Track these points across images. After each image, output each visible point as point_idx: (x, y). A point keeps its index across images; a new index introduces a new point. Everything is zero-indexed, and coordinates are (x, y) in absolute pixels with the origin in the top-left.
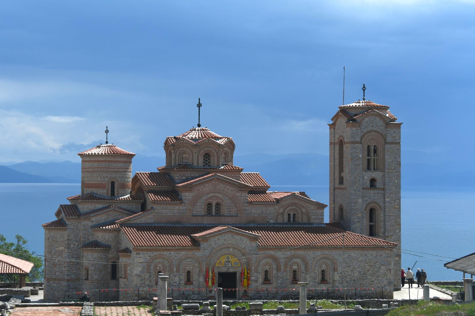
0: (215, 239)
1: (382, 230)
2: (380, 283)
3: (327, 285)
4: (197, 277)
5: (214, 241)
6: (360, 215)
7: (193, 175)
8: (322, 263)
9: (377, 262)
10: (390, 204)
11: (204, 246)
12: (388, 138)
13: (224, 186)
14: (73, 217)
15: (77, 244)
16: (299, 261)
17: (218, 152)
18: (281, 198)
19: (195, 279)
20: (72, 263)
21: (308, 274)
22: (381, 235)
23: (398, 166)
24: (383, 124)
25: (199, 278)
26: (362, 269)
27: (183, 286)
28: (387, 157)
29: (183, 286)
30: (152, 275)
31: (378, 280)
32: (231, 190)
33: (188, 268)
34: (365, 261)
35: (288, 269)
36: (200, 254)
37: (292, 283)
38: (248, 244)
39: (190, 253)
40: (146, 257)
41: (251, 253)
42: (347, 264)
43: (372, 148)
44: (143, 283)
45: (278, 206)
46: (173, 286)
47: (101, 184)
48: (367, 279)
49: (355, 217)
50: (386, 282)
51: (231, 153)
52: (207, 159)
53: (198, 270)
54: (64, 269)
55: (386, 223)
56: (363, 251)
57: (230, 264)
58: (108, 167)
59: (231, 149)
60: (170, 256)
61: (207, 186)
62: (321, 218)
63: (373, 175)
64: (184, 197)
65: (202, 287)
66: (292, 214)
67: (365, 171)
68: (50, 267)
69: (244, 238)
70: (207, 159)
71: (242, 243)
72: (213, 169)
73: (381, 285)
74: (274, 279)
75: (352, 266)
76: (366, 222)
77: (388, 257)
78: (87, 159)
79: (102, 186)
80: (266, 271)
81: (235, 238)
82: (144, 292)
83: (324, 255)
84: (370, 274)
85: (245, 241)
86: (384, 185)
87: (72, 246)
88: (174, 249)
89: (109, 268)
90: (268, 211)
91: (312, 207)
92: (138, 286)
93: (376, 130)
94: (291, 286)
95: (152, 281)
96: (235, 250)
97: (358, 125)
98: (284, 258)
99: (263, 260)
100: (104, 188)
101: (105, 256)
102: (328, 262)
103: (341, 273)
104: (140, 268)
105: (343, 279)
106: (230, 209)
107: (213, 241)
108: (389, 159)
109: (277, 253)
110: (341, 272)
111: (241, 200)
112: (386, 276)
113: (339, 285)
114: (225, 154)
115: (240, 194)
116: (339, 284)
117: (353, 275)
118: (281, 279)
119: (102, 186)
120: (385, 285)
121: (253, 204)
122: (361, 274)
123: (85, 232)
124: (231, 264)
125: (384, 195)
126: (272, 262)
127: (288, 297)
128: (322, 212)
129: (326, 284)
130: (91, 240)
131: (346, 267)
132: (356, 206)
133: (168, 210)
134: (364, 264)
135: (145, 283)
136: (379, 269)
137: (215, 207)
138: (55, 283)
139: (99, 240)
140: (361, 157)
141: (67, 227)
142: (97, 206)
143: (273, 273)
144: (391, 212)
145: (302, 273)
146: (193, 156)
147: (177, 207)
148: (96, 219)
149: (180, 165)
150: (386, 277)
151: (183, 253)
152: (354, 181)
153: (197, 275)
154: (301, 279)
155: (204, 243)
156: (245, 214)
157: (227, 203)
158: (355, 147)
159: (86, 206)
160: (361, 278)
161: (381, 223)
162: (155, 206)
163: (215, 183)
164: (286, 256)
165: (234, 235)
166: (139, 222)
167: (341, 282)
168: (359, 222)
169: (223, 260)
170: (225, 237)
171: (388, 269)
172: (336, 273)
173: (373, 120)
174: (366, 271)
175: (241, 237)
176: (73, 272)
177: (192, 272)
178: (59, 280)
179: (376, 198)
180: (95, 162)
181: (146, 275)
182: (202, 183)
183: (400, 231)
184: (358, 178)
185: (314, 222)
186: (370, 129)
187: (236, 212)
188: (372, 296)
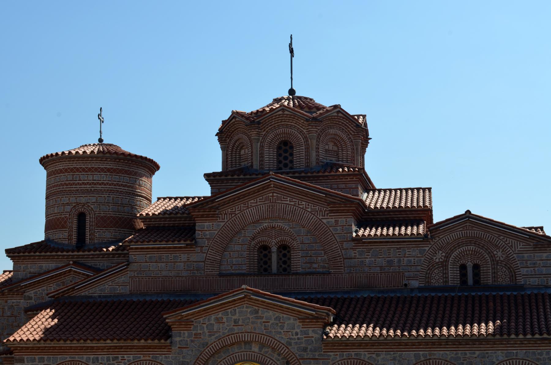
0: (209, 320)
5: (207, 327)
11: (182, 339)
13: (292, 203)
17: (308, 136)
36: (170, 360)
39: (148, 358)
41: (305, 357)
45: (430, 246)
47: (58, 219)
51: (352, 141)
58: (72, 182)
59: (351, 132)
61: (253, 205)
62: (544, 273)
64: (200, 232)
66: (470, 266)
69: (285, 316)
70: (287, 155)
71: (282, 329)
83: (514, 361)
90: (405, 259)
91: (520, 246)
96: (266, 350)
100: (63, 227)
106: (311, 256)
107: (205, 326)
109: (378, 355)
111: (335, 235)
114: (335, 143)
121: (364, 243)
123: (14, 322)
133: (163, 264)
137: (278, 255)
142: (44, 265)
148: (36, 293)
151: (128, 357)
155: (182, 332)
159: (22, 267)
162: (133, 256)
163: (273, 196)
165: (260, 309)
175: (277, 314)
187: (326, 265)
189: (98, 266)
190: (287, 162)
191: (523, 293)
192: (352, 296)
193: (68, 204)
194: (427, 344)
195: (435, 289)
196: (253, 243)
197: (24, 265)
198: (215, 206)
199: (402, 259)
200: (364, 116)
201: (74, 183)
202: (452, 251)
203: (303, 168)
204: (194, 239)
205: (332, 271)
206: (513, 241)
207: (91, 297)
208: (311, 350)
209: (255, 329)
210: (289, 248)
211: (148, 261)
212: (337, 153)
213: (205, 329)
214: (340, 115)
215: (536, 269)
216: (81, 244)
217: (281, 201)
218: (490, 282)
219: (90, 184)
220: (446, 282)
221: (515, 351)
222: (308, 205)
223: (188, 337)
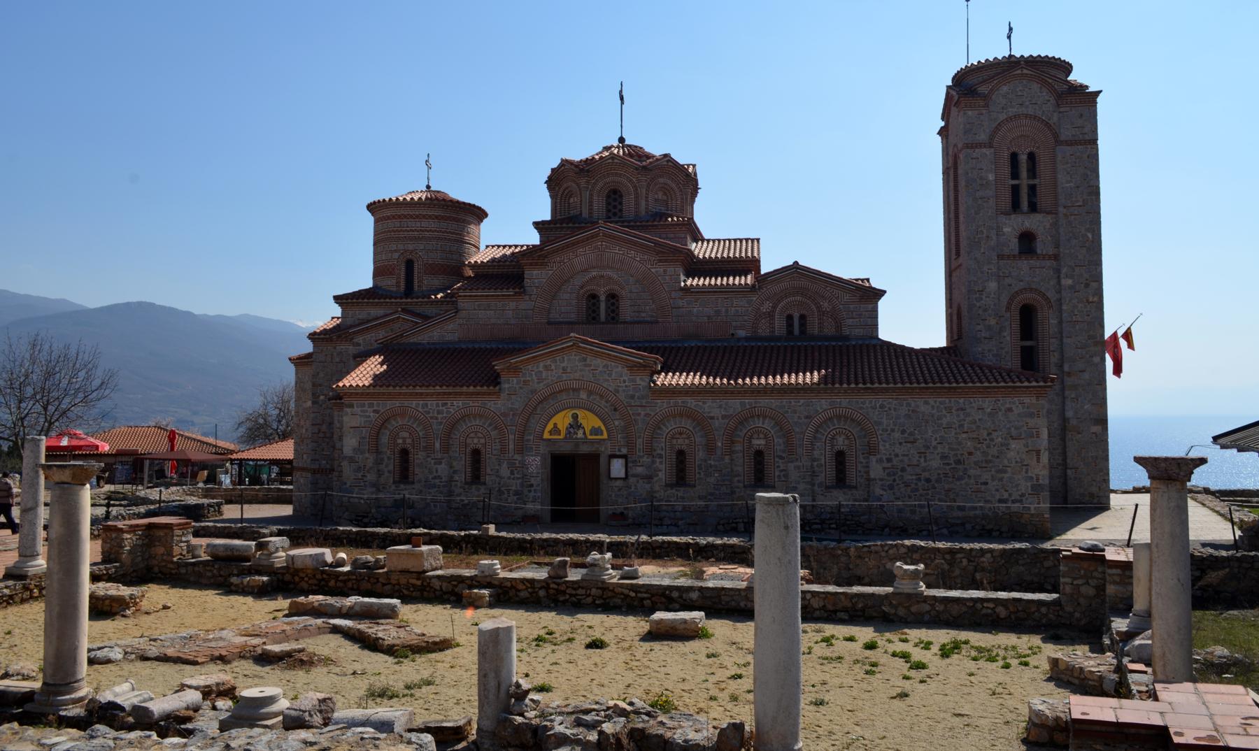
0: (538, 367)
1: (1054, 358)
2: (1007, 489)
3: (850, 493)
6: (993, 322)
9: (996, 431)
12: (1062, 131)
16: (767, 425)
20: (321, 435)
21: (792, 462)
26: (951, 449)
27: (461, 487)
29: (461, 487)
30: (386, 459)
33: (475, 442)
35: (738, 447)
36: (499, 406)
38: (624, 382)
39: (477, 404)
42: (906, 435)
43: (1023, 158)
46: (434, 486)
48: (966, 476)
49: (979, 327)
50: (1025, 486)
53: (499, 447)
55: (1065, 340)
56: (953, 400)
63: (1026, 223)
65: (506, 492)
66: (796, 316)
70: (617, 203)
73: (1010, 495)
74: (699, 473)
75: (920, 441)
77: (1031, 415)
80: (681, 453)
81: (590, 365)
82: (362, 501)
84: (976, 463)
85: (616, 372)
86: (1057, 246)
87: (322, 397)
90: (733, 309)
94: (748, 492)
95: (386, 474)
97: (982, 103)
98: (723, 419)
100: (391, 274)
103: (889, 460)
104: (354, 440)
105: (894, 474)
108: (1068, 182)
109: (704, 403)
110: (888, 456)
113: (881, 492)
116: (883, 489)
120: (1023, 495)
121: (692, 292)
122: (948, 464)
124: (584, 433)
125: (1058, 271)
126: (694, 428)
127: (736, 523)
132: (982, 299)
134: (956, 434)
135: (365, 479)
136: (1004, 448)
137: (606, 304)
145: (777, 459)
147: (513, 305)
150: (1027, 472)
152: (975, 238)
157: (631, 292)
158: (975, 155)
161: (1052, 340)
164: (731, 413)
167: (888, 483)
169: (562, 420)
170: (564, 361)
171: (1030, 448)
172: (873, 459)
173: (1021, 88)
175: (605, 362)
179: (1035, 280)
181: (367, 458)
184: (985, 231)
188: (983, 526)
190: (617, 211)
191: (848, 343)
192: (680, 345)
193: (395, 251)
194: (753, 392)
200: (694, 166)
202: (779, 302)
204: (523, 287)
207: (420, 344)
208: (638, 398)
209: (583, 377)
214: (670, 164)
216: (409, 291)
218: (816, 332)
220: (773, 332)
223: (517, 384)
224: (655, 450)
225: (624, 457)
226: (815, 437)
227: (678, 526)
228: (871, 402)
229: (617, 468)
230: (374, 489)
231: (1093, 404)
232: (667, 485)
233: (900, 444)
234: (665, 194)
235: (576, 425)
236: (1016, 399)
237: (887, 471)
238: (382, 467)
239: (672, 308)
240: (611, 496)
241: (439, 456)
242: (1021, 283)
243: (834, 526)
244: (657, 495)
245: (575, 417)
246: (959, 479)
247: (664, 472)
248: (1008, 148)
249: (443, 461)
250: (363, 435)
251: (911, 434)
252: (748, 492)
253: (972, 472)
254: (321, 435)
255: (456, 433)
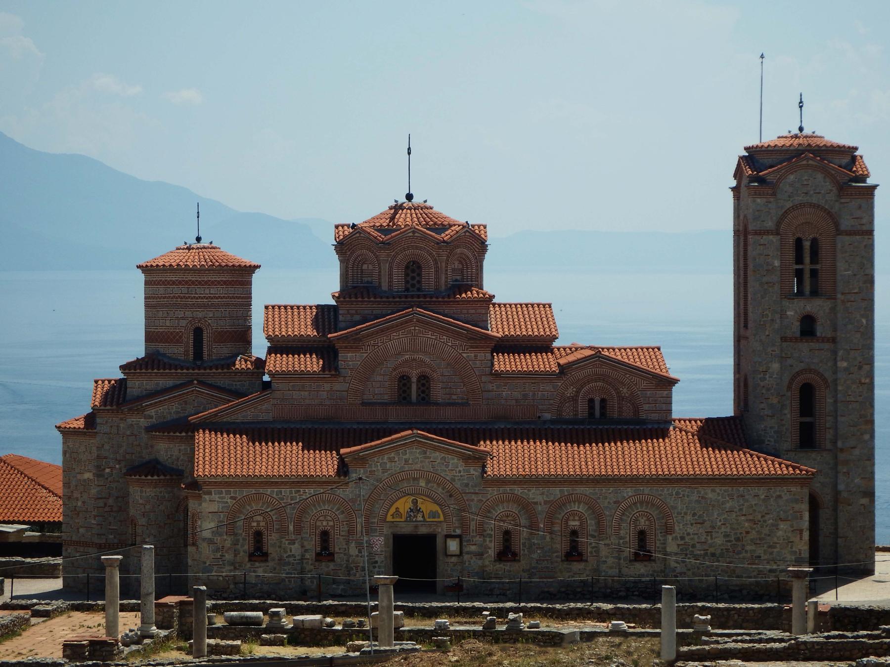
0: (382, 459)
4: (344, 544)
6: (775, 401)
7: (379, 312)
8: (637, 514)
9: (768, 514)
10: (849, 374)
14: (107, 408)
15: (117, 466)
18: (569, 363)
19: (340, 549)
20: (107, 509)
22: (829, 446)
23: (869, 285)
24: (833, 188)
25: (348, 548)
27: (311, 564)
28: (841, 265)
29: (311, 564)
31: (771, 553)
32: (451, 346)
33: (324, 525)
34: (741, 510)
37: (567, 560)
40: (226, 500)
41: (467, 491)
42: (696, 517)
43: (807, 244)
44: (219, 557)
46: (289, 563)
47: (172, 333)
48: (744, 551)
49: (762, 406)
51: (476, 258)
52: (415, 275)
54: (93, 522)
55: (839, 418)
57: (420, 515)
58: (187, 295)
59: (476, 249)
60: (279, 498)
61: (395, 338)
64: (343, 362)
65: (354, 568)
66: (597, 400)
67: (789, 299)
68: (68, 515)
69: (450, 456)
70: (415, 275)
72: (425, 296)
74: (524, 550)
76: (790, 416)
77: (796, 501)
78: (157, 278)
79: (174, 337)
82: (221, 578)
83: (641, 496)
84: (752, 540)
85: (452, 464)
86: (835, 330)
87: (108, 470)
88: (288, 482)
89: (180, 521)
90: (540, 393)
91: (644, 384)
92: (207, 564)
93: (816, 202)
95: (242, 553)
99: (496, 508)
100: (178, 341)
101: (171, 494)
102: (651, 513)
103: (682, 538)
105: (686, 550)
106: (450, 388)
107: (379, 464)
108: (846, 270)
109: (529, 490)
112: (790, 546)
113: (676, 565)
114: (460, 261)
115: (473, 355)
117: (710, 541)
118: (538, 552)
119: (174, 337)
122: (730, 541)
124: (423, 517)
125: (835, 353)
126: (519, 512)
128: (667, 395)
129: (646, 563)
130: (147, 458)
131: (694, 525)
133: (307, 393)
134: (736, 516)
136: (774, 528)
137: (417, 385)
138: (78, 550)
139: (161, 459)
140: (776, 265)
141: (95, 429)
142: (161, 382)
143: (521, 536)
144: (850, 394)
146: (380, 268)
147: (327, 386)
149: (355, 287)
152: (760, 321)
153: (344, 539)
154: (589, 551)
156: (484, 401)
158: (762, 242)
160: (731, 550)
163: (415, 330)
166: (240, 418)
168: (772, 416)
169: (404, 505)
171: (795, 528)
172: (670, 537)
173: (806, 178)
174: (741, 533)
175: (443, 455)
176: (111, 527)
177: (332, 532)
178: (86, 544)
180: (161, 285)
181: (225, 540)
182: (382, 330)
183: (872, 437)
184: (770, 315)
185: (649, 418)
186: (801, 200)
189: (219, 384)
190: (415, 282)
191: (645, 427)
192: (490, 427)
193: (183, 318)
194: (571, 482)
195: (567, 422)
196: (394, 374)
197: (139, 382)
198: (359, 338)
199: (536, 393)
200: (485, 227)
201: (189, 297)
202: (582, 387)
203: (432, 291)
204: (336, 369)
205: (471, 402)
206: (638, 379)
207: (234, 423)
209: (423, 467)
210: (428, 377)
211: (291, 389)
212: (462, 271)
213: (379, 467)
215: (657, 405)
217: (423, 334)
218: (616, 416)
219: (207, 299)
221: (642, 488)
222: (449, 340)
223: (364, 473)
224: (485, 531)
225: (459, 537)
226: (621, 519)
227: (506, 596)
228: (668, 490)
229: (453, 546)
230: (232, 568)
231: (862, 478)
232: (495, 561)
233: (692, 524)
234: (461, 262)
235: (415, 510)
236: (785, 488)
237: (681, 547)
238: (239, 547)
239: (482, 391)
240: (446, 571)
241: (293, 537)
242: (802, 364)
243: (636, 593)
244: (487, 569)
245: (415, 502)
246: (739, 553)
247: (493, 548)
248: (794, 234)
249: (296, 542)
250: (221, 519)
251: (700, 516)
252: (565, 566)
253: (748, 548)
254: (107, 509)
255: (308, 516)
